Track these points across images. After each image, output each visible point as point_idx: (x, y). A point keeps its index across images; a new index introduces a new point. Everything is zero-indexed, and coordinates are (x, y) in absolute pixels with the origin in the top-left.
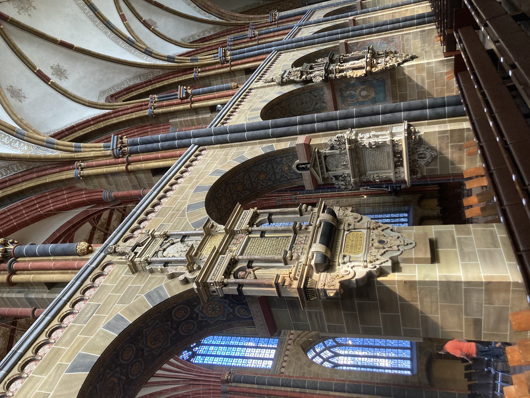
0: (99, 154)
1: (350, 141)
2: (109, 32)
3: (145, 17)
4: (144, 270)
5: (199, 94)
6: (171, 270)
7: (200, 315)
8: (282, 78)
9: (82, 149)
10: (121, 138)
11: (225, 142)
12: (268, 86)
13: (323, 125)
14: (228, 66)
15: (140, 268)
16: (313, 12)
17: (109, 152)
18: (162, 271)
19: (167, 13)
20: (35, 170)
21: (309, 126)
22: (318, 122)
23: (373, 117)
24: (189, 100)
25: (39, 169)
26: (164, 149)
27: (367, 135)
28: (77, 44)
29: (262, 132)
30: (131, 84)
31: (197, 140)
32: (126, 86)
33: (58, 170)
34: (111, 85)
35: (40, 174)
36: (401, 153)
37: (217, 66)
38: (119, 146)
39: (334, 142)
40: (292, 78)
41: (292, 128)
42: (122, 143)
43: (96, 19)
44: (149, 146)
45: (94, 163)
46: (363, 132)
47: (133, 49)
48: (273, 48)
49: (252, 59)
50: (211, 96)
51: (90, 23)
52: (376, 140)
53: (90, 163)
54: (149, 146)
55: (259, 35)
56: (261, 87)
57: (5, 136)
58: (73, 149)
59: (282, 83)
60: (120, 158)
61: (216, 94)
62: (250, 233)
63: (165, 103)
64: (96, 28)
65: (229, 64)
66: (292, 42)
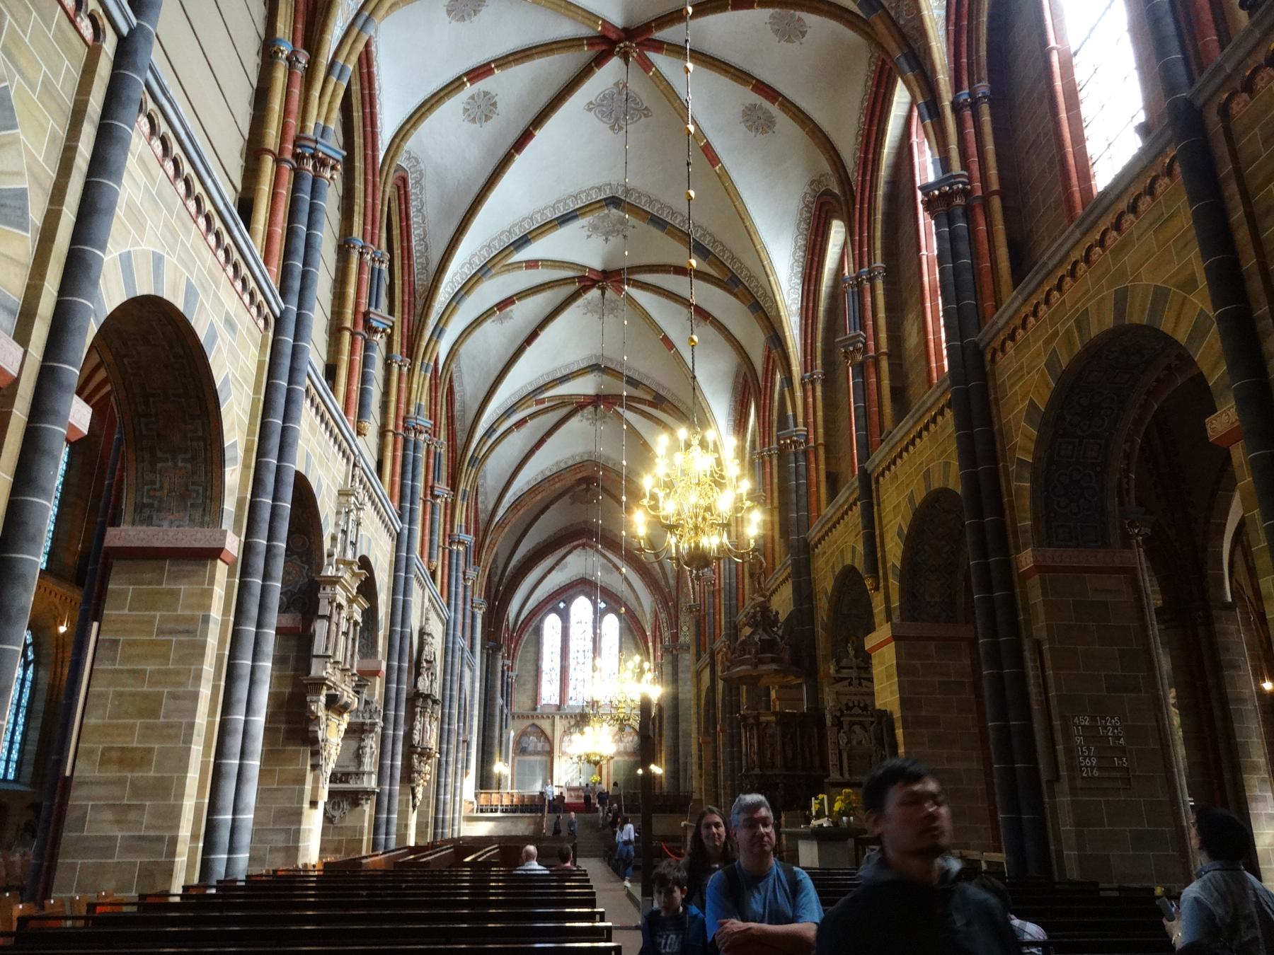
1: (374, 725)
2: (530, 389)
3: (530, 423)
4: (340, 504)
5: (433, 513)
6: (340, 535)
8: (429, 635)
10: (426, 432)
11: (396, 569)
12: (422, 613)
13: (393, 694)
15: (343, 499)
16: (472, 670)
17: (412, 409)
18: (337, 524)
20: (412, 299)
21: (395, 677)
23: (390, 753)
24: (429, 498)
25: (412, 306)
26: (402, 486)
27: (374, 746)
28: (530, 350)
29: (399, 618)
30: (457, 397)
31: (406, 532)
32: (456, 389)
33: (405, 330)
34: (464, 369)
35: (406, 304)
36: (347, 782)
37: (448, 527)
39: (374, 706)
40: (426, 648)
41: (396, 656)
42: (421, 432)
43: (551, 378)
44: (410, 468)
45: (404, 385)
47: (500, 413)
49: (446, 581)
50: (427, 531)
52: (368, 755)
53: (405, 379)
54: (410, 468)
56: (423, 603)
57: (463, 279)
58: (426, 361)
59: (422, 633)
60: (404, 422)
61: (427, 538)
62: (348, 620)
63: (432, 461)
64: (540, 373)
65: (447, 546)
66: (454, 643)
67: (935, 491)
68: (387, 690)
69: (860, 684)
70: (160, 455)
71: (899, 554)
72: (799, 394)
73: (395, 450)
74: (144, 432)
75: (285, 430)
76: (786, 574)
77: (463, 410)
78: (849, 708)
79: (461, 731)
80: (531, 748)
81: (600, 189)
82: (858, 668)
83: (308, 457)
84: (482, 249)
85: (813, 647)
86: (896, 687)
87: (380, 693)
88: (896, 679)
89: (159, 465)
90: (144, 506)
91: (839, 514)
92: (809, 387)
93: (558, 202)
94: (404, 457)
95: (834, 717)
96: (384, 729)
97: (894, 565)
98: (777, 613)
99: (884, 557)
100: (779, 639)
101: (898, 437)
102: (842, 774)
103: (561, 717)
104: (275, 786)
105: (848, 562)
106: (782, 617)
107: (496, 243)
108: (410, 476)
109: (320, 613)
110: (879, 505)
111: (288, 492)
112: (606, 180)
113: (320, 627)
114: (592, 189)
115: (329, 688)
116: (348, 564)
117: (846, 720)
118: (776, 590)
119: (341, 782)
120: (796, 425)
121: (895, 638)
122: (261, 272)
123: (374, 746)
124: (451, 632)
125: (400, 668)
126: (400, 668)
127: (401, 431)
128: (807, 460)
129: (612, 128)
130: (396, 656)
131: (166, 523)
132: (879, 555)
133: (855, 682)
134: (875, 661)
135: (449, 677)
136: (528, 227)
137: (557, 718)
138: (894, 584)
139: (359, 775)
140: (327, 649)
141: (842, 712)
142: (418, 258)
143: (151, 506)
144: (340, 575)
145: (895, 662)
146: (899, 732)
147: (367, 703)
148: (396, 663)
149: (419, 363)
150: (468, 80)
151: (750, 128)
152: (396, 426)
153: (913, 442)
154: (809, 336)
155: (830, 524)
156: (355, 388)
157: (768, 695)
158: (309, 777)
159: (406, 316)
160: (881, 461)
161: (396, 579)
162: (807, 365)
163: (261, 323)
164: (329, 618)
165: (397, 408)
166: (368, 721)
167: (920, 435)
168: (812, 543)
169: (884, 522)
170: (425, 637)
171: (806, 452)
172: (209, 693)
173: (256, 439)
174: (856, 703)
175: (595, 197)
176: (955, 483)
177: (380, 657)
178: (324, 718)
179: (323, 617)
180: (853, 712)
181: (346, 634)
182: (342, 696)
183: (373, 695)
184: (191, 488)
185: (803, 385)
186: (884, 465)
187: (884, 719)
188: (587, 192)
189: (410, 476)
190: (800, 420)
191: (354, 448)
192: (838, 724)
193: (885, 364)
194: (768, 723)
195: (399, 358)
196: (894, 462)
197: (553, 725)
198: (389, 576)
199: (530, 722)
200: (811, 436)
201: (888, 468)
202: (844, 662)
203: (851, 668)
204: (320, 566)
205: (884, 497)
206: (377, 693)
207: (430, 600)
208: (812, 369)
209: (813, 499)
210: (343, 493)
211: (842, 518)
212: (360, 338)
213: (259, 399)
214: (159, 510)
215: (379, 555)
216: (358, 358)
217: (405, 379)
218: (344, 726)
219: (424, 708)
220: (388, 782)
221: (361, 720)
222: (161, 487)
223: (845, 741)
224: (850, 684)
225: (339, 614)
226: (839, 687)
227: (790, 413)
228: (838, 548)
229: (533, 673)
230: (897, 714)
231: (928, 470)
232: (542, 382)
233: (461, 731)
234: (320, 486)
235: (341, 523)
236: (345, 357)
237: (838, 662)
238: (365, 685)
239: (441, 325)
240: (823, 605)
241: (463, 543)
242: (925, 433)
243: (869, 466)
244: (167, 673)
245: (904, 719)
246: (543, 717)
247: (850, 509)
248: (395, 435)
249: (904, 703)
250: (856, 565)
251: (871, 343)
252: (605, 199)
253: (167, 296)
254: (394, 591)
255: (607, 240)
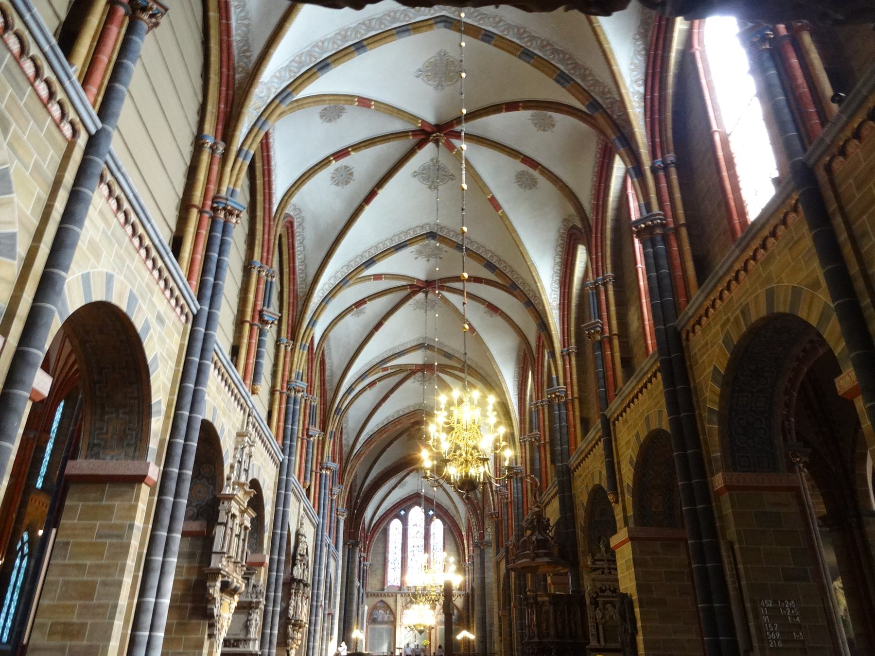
0: (294, 367)
1: (258, 603)
2: (378, 360)
3: (378, 384)
4: (237, 443)
5: (308, 448)
6: (236, 465)
7: (198, 482)
8: (302, 535)
9: (301, 351)
11: (279, 488)
13: (273, 580)
14: (316, 469)
15: (240, 439)
16: (336, 560)
17: (293, 375)
18: (234, 457)
19: (375, 404)
20: (295, 301)
22: (277, 576)
23: (269, 625)
24: (305, 437)
25: (295, 305)
26: (285, 429)
27: (258, 619)
29: (280, 524)
30: (327, 366)
31: (286, 462)
32: (327, 361)
33: (290, 322)
34: (332, 348)
35: (291, 305)
36: (237, 646)
37: (320, 457)
38: (297, 388)
39: (259, 589)
40: (300, 545)
41: (276, 552)
42: (299, 391)
44: (291, 416)
45: (288, 359)
46: (260, 617)
47: (357, 377)
48: (321, 520)
49: (317, 496)
50: (303, 461)
51: (391, 347)
52: (254, 626)
53: (289, 355)
54: (291, 416)
55: (332, 500)
58: (304, 343)
59: (298, 534)
60: (288, 385)
61: (303, 465)
62: (240, 526)
63: (308, 411)
64: (384, 350)
65: (318, 470)
67: (654, 430)
68: (269, 577)
69: (610, 573)
70: (107, 409)
71: (631, 477)
72: (560, 362)
73: (280, 404)
74: (98, 393)
75: (195, 392)
76: (555, 491)
77: (332, 376)
78: (602, 591)
79: (327, 606)
80: (380, 619)
81: (422, 227)
82: (608, 561)
83: (215, 410)
84: (344, 266)
85: (575, 545)
86: (633, 576)
87: (264, 579)
88: (633, 570)
89: (106, 417)
90: (95, 445)
91: (589, 447)
92: (567, 358)
93: (395, 236)
94: (287, 408)
95: (592, 598)
96: (266, 606)
97: (628, 485)
98: (549, 520)
99: (621, 479)
100: (550, 539)
101: (627, 392)
102: (599, 642)
103: (402, 595)
104: (181, 650)
105: (597, 482)
106: (552, 523)
107: (352, 263)
108: (290, 421)
109: (220, 521)
110: (616, 440)
111: (196, 435)
112: (426, 221)
113: (219, 531)
114: (417, 227)
115: (224, 576)
116: (241, 485)
117: (600, 600)
118: (549, 502)
119: (234, 646)
120: (558, 385)
121: (631, 538)
122: (184, 284)
123: (258, 619)
124: (320, 533)
125: (279, 560)
126: (279, 560)
127: (285, 390)
128: (567, 409)
129: (430, 188)
130: (276, 552)
131: (108, 458)
132: (617, 477)
133: (606, 571)
134: (618, 556)
135: (317, 566)
136: (374, 252)
137: (399, 596)
138: (629, 498)
139: (246, 641)
140: (223, 547)
141: (597, 594)
142: (300, 274)
143: (99, 445)
144: (235, 493)
145: (631, 557)
146: (637, 610)
147: (254, 586)
148: (276, 557)
149: (299, 344)
150: (334, 159)
151: (520, 186)
152: (282, 387)
153: (636, 396)
154: (566, 323)
155: (584, 454)
156: (251, 361)
157: (545, 580)
158: (206, 644)
159: (291, 312)
160: (616, 410)
161: (278, 495)
162: (565, 343)
163: (183, 318)
164: (225, 525)
165: (283, 375)
166: (254, 600)
167: (641, 391)
168: (572, 468)
169: (620, 453)
170: (300, 537)
171: (566, 403)
172: (130, 581)
173: (176, 398)
174: (608, 587)
175: (419, 232)
176: (666, 426)
177: (265, 552)
178: (219, 599)
179: (221, 524)
180: (606, 594)
181: (238, 536)
182: (233, 582)
183: (259, 581)
184: (127, 432)
185: (563, 356)
186: (618, 412)
187: (625, 597)
188: (414, 229)
189: (290, 421)
190: (561, 381)
191: (249, 402)
192: (595, 603)
193: (616, 342)
194: (543, 602)
195: (285, 340)
196: (625, 411)
197: (396, 601)
198: (274, 493)
199: (380, 599)
200: (569, 392)
201: (621, 415)
202: (598, 556)
203: (603, 560)
204: (221, 487)
205: (619, 436)
206: (262, 579)
207: (304, 510)
208: (568, 346)
209: (572, 437)
210: (240, 435)
211: (592, 450)
212: (256, 327)
213: (179, 370)
214: (104, 448)
215: (267, 480)
216: (254, 341)
217: (289, 355)
218: (234, 604)
219: (298, 590)
220: (267, 646)
221: (249, 599)
222: (107, 433)
223: (600, 617)
224: (603, 573)
225: (233, 521)
226: (594, 575)
227: (554, 376)
228: (589, 473)
229: (381, 562)
230: (635, 597)
231: (648, 416)
232: (386, 356)
233: (327, 606)
234: (223, 430)
235: (238, 456)
236: (245, 341)
237: (593, 556)
238: (253, 573)
239: (314, 318)
240: (581, 513)
241: (330, 469)
242: (644, 390)
243: (608, 413)
244: (101, 566)
245: (640, 600)
246: (388, 595)
247: (597, 443)
248: (281, 393)
249: (639, 587)
250: (602, 485)
251: (606, 328)
252: (426, 234)
253: (115, 301)
254: (277, 504)
255: (428, 260)
